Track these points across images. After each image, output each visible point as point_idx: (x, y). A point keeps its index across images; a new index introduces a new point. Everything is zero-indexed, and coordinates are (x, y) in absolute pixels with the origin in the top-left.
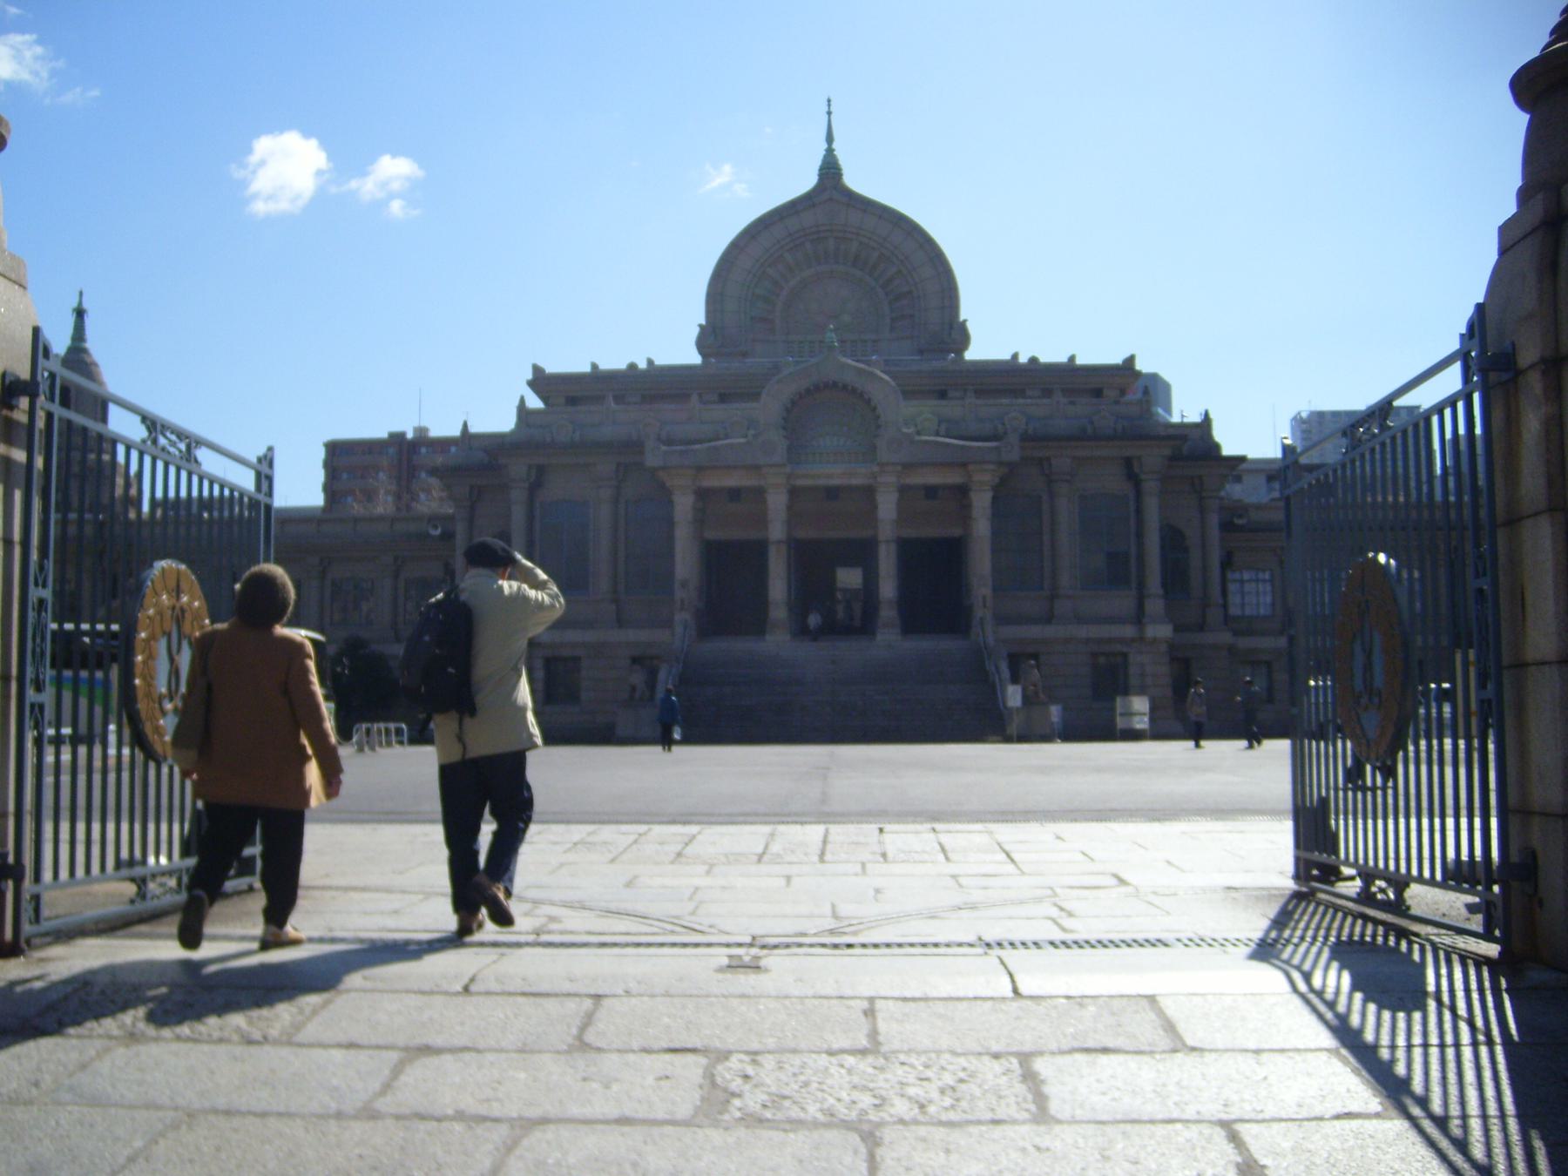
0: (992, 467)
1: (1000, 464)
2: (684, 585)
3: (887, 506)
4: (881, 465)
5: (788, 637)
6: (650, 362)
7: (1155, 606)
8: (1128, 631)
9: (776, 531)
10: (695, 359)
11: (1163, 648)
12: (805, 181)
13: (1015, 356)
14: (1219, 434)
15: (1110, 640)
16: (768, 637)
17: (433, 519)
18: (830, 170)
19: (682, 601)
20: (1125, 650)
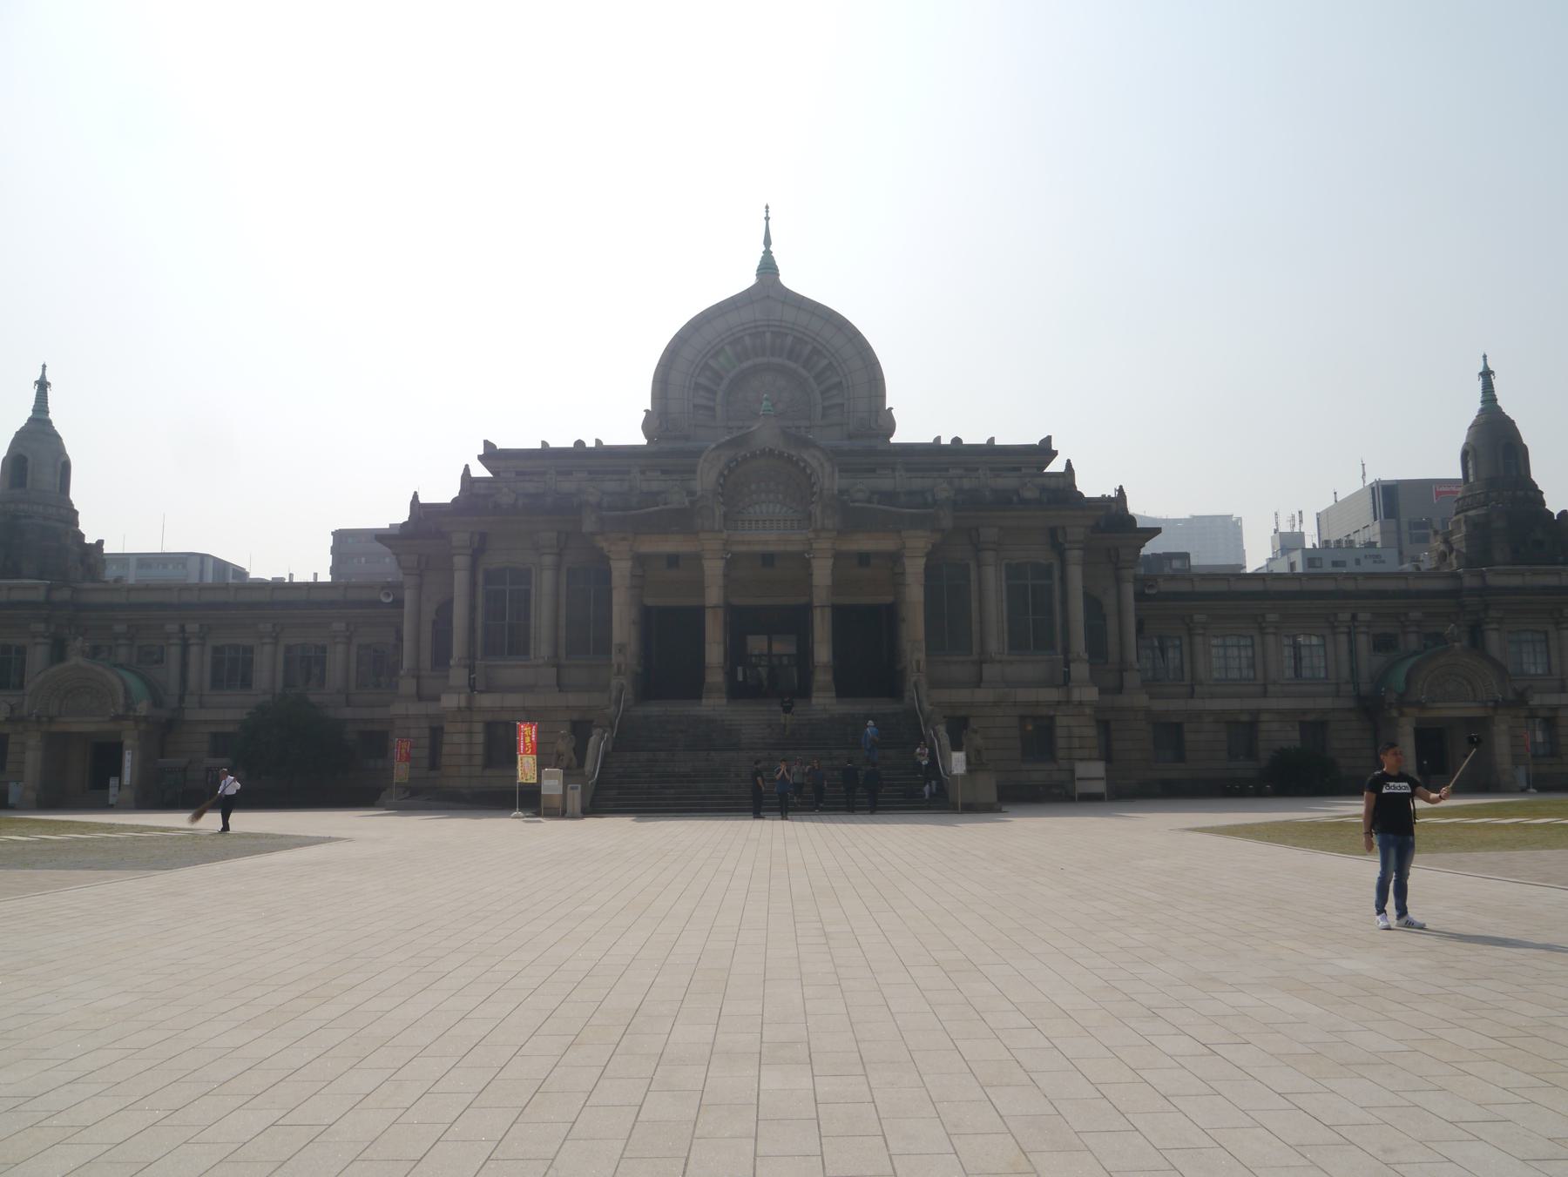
2: (622, 648)
3: (822, 573)
5: (724, 701)
6: (598, 441)
7: (1080, 670)
9: (713, 595)
10: (644, 442)
12: (745, 279)
13: (938, 439)
14: (1134, 507)
16: (704, 701)
17: (388, 587)
18: (768, 268)
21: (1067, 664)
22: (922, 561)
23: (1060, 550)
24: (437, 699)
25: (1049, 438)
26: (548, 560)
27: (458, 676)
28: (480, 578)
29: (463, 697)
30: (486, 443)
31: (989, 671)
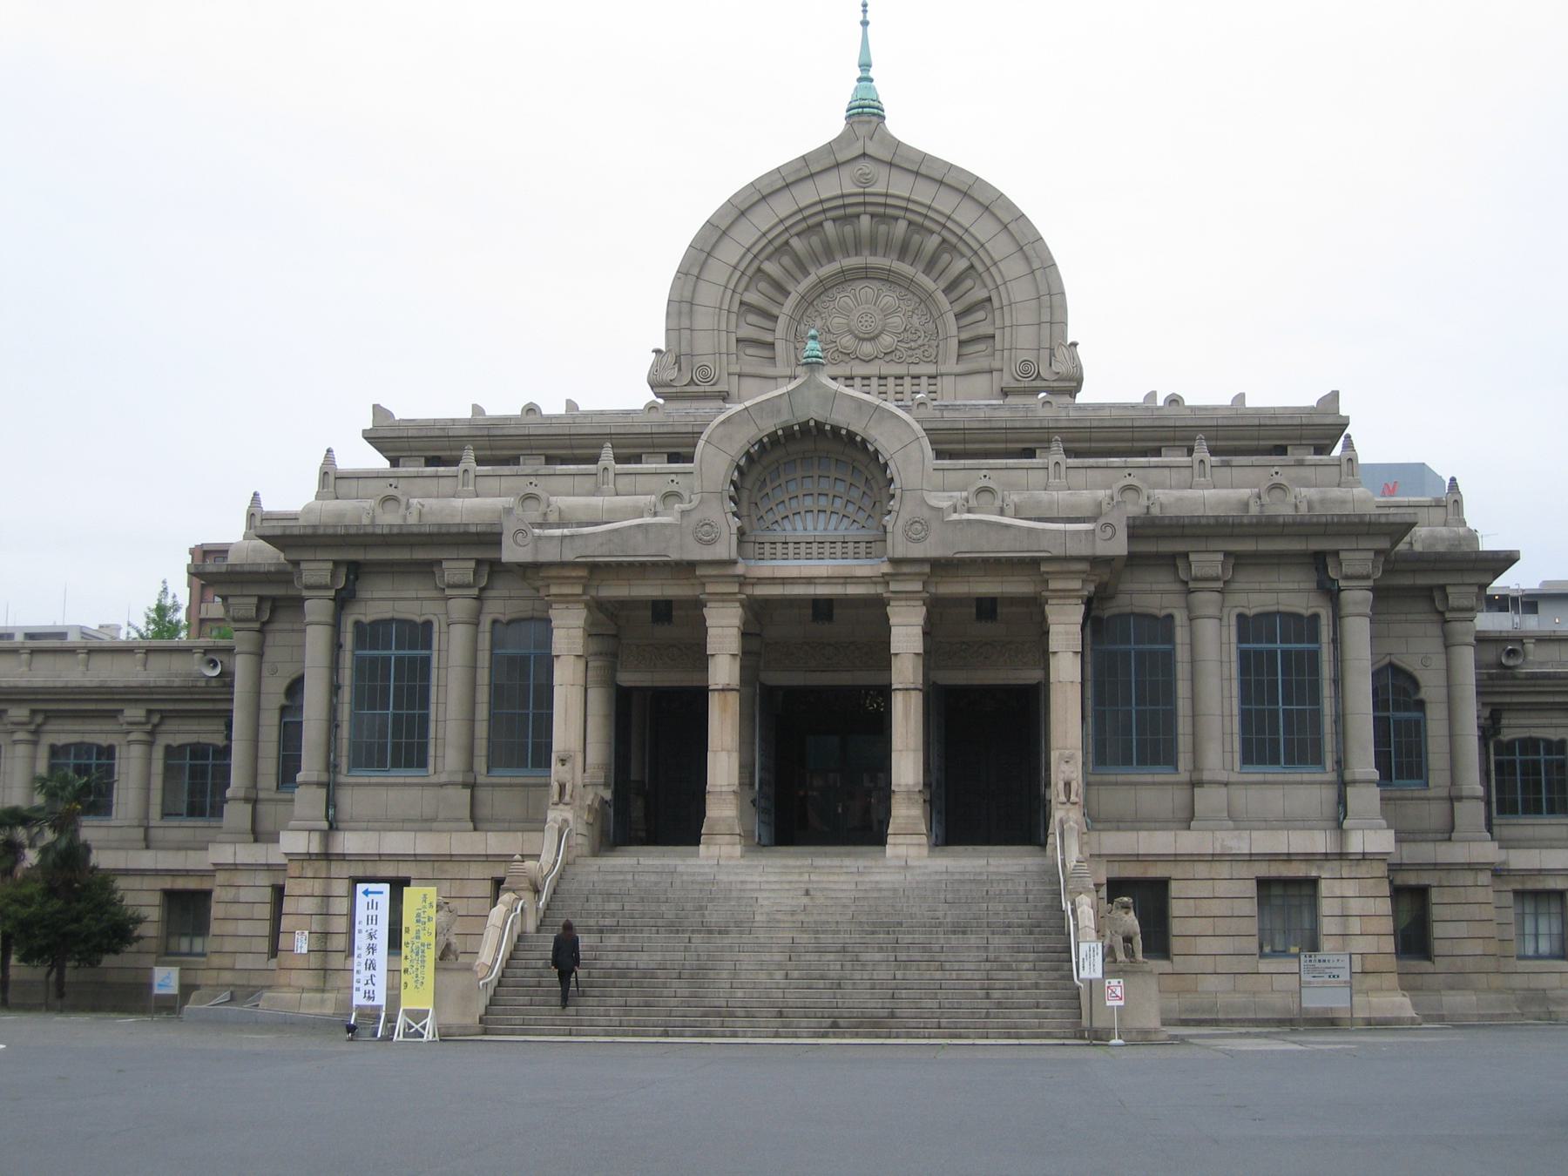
0: (1084, 566)
1: (1096, 561)
3: (906, 635)
4: (895, 562)
5: (738, 850)
6: (571, 405)
8: (1320, 842)
9: (723, 670)
11: (1380, 870)
15: (1289, 858)
19: (562, 787)
20: (1314, 874)
21: (1342, 784)
22: (1077, 613)
23: (1331, 593)
24: (277, 841)
25: (1335, 395)
26: (460, 606)
27: (308, 800)
28: (348, 639)
29: (316, 837)
30: (377, 409)
31: (1207, 799)
